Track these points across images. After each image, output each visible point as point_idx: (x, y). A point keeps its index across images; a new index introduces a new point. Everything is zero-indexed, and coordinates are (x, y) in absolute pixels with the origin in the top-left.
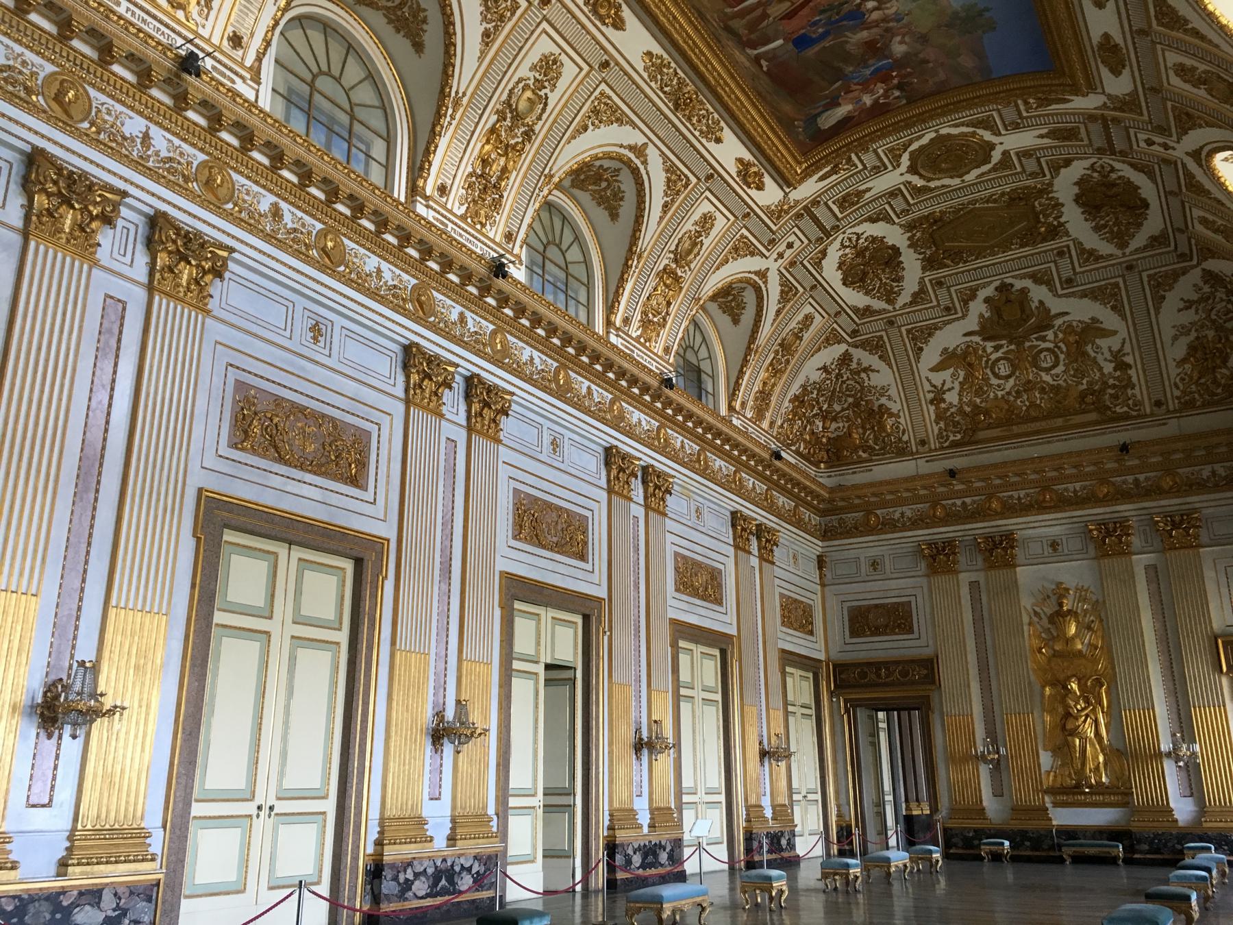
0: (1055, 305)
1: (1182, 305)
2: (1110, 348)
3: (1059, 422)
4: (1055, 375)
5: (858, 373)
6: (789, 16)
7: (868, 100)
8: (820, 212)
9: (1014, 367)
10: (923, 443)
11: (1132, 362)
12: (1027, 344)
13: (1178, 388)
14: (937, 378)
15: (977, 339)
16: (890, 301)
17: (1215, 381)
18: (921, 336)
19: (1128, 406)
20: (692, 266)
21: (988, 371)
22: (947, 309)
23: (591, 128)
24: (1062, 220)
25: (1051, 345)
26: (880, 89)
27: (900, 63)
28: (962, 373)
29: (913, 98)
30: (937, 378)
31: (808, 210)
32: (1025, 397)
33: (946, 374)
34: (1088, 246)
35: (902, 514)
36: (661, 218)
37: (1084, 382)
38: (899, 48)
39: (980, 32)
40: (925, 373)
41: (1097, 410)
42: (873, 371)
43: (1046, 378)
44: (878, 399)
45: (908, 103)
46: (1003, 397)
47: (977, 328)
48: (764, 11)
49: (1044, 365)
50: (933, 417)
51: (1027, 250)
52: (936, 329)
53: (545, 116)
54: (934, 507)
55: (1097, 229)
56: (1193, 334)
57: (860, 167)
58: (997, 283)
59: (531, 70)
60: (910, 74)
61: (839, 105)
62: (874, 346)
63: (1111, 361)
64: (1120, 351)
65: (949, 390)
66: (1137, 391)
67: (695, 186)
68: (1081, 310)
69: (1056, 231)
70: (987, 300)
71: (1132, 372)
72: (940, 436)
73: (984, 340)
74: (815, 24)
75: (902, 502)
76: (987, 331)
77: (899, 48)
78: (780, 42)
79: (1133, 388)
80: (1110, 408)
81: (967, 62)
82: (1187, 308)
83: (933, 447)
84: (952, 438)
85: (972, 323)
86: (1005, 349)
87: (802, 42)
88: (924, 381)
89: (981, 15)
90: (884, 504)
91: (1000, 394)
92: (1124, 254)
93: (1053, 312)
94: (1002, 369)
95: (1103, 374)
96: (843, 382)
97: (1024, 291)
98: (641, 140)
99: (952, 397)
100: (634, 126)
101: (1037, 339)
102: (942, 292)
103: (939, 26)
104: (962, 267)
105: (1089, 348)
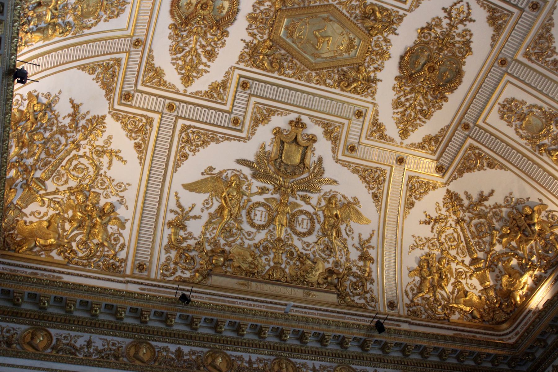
0: (331, 169)
1: (424, 218)
2: (360, 235)
3: (299, 293)
4: (307, 244)
5: (101, 153)
9: (272, 220)
10: (141, 267)
11: (375, 258)
12: (291, 199)
13: (407, 295)
14: (189, 199)
15: (247, 171)
16: (187, 80)
17: (435, 299)
18: (195, 139)
19: (365, 298)
21: (244, 213)
22: (236, 121)
24: (379, 75)
25: (311, 210)
28: (216, 205)
30: (189, 199)
32: (272, 256)
33: (199, 198)
34: (381, 119)
35: (89, 343)
37: (331, 260)
40: (177, 186)
41: (340, 296)
42: (120, 159)
43: (297, 243)
44: (107, 196)
46: (250, 246)
47: (251, 158)
49: (299, 229)
50: (165, 241)
51: (336, 93)
52: (213, 139)
54: (137, 345)
55: (397, 104)
56: (426, 250)
58: (293, 117)
62: (138, 130)
63: (357, 249)
64: (368, 241)
65: (195, 217)
66: (374, 287)
68: (348, 185)
69: (370, 83)
70: (278, 132)
71: (373, 267)
72: (166, 267)
73: (254, 176)
75: (93, 325)
76: (261, 167)
79: (372, 282)
80: (350, 296)
82: (427, 223)
83: (153, 276)
84: (179, 273)
85: (250, 150)
86: (268, 196)
88: (172, 194)
90: (67, 322)
91: (247, 242)
92: (401, 143)
93: (327, 175)
94: (258, 218)
95: (348, 260)
96: (75, 157)
97: (313, 139)
99: (195, 228)
101: (303, 198)
102: (242, 95)
104: (274, 78)
105: (343, 227)
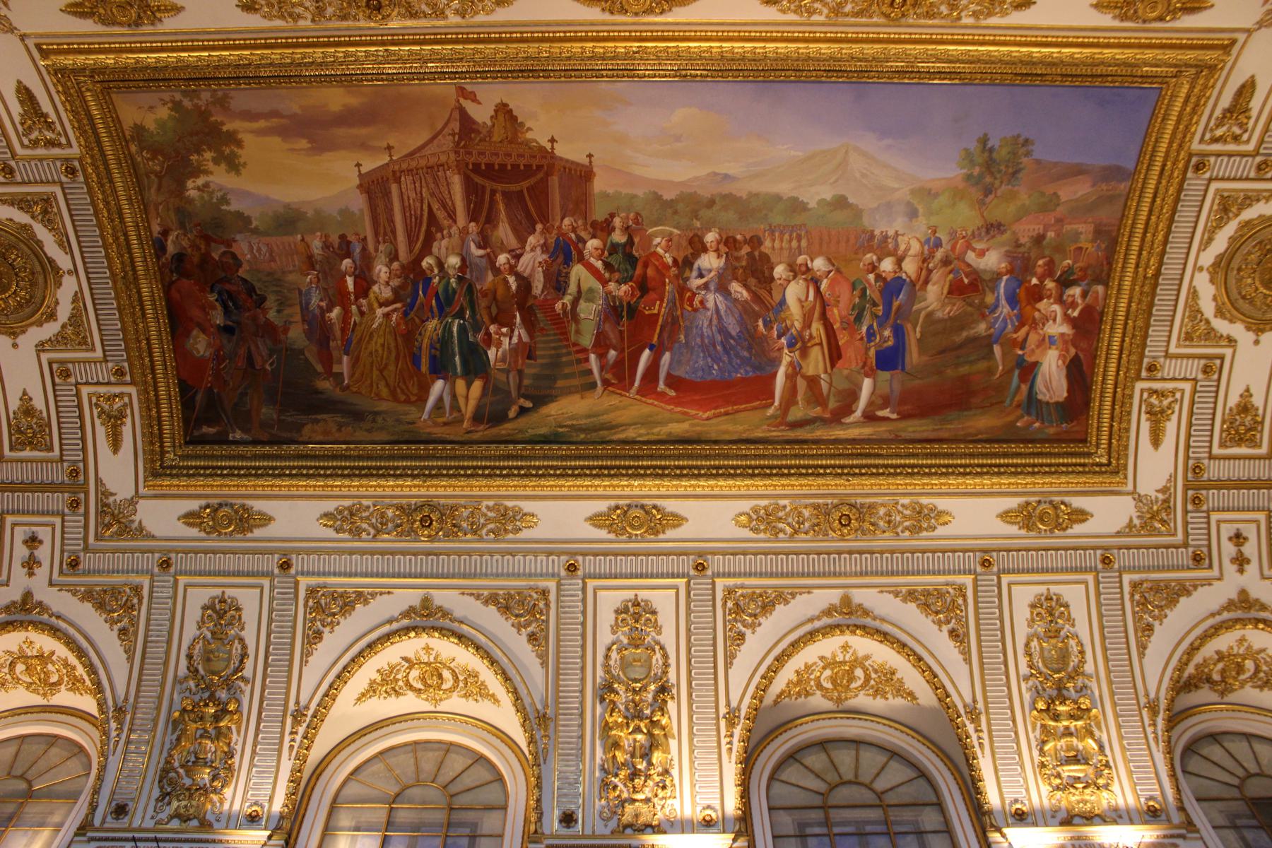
6: (835, 355)
7: (1058, 328)
8: (1214, 471)
20: (1089, 668)
23: (748, 632)
26: (1048, 306)
27: (1020, 266)
29: (1102, 273)
31: (1196, 481)
36: (966, 654)
38: (991, 260)
39: (1025, 160)
45: (1106, 285)
48: (804, 377)
53: (672, 661)
57: (1187, 387)
59: (614, 633)
60: (1051, 265)
61: (1035, 365)
67: (976, 586)
74: (871, 334)
77: (991, 260)
78: (867, 384)
81: (1075, 191)
87: (889, 360)
89: (991, 150)
98: (834, 596)
100: (809, 589)
103: (982, 203)
